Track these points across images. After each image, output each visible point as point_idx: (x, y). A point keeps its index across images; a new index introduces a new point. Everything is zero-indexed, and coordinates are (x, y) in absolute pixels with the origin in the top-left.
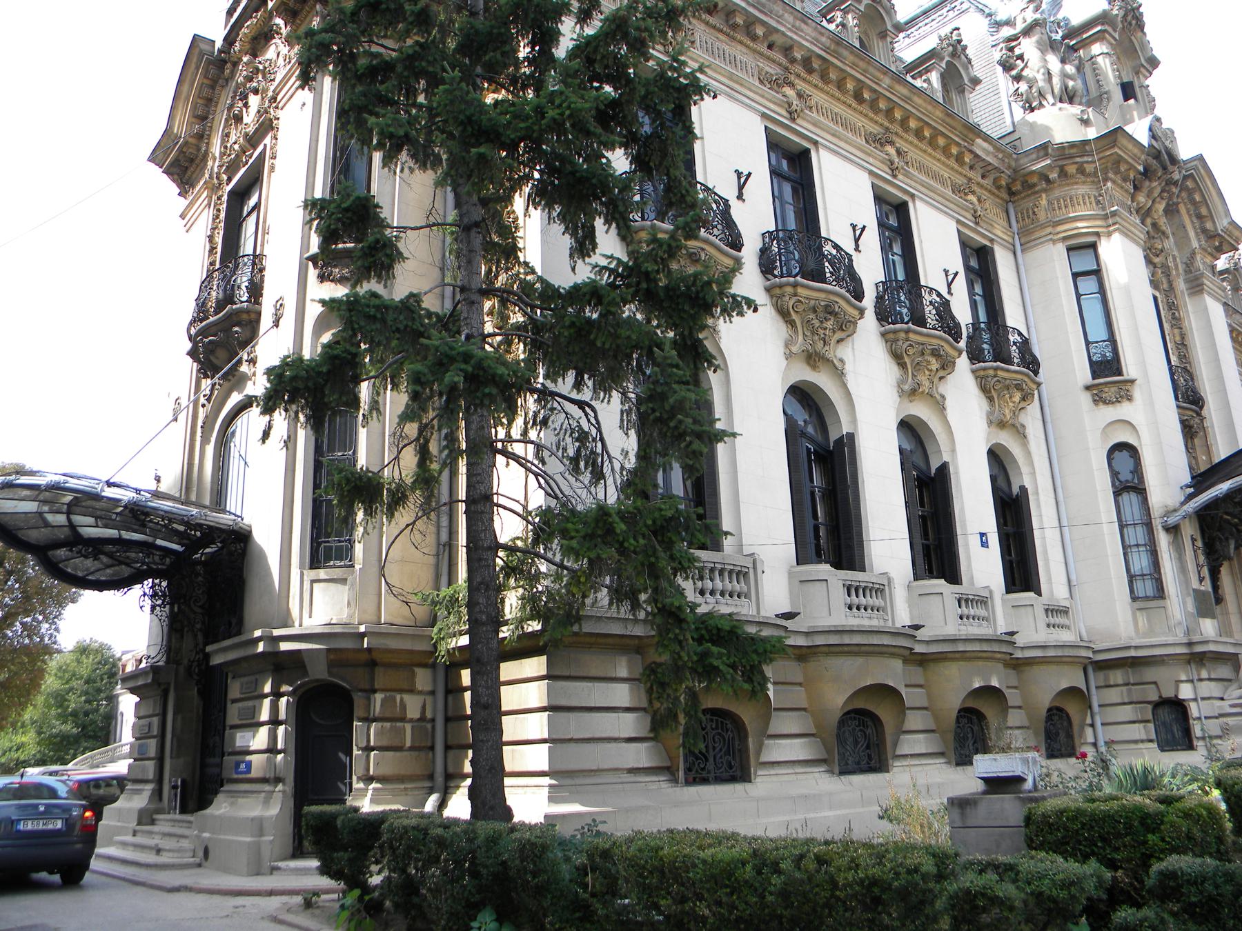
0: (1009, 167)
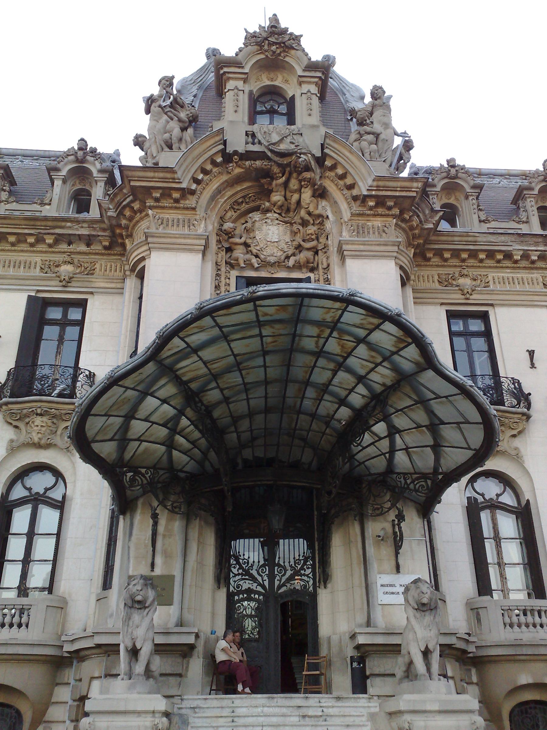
0: (104, 230)
